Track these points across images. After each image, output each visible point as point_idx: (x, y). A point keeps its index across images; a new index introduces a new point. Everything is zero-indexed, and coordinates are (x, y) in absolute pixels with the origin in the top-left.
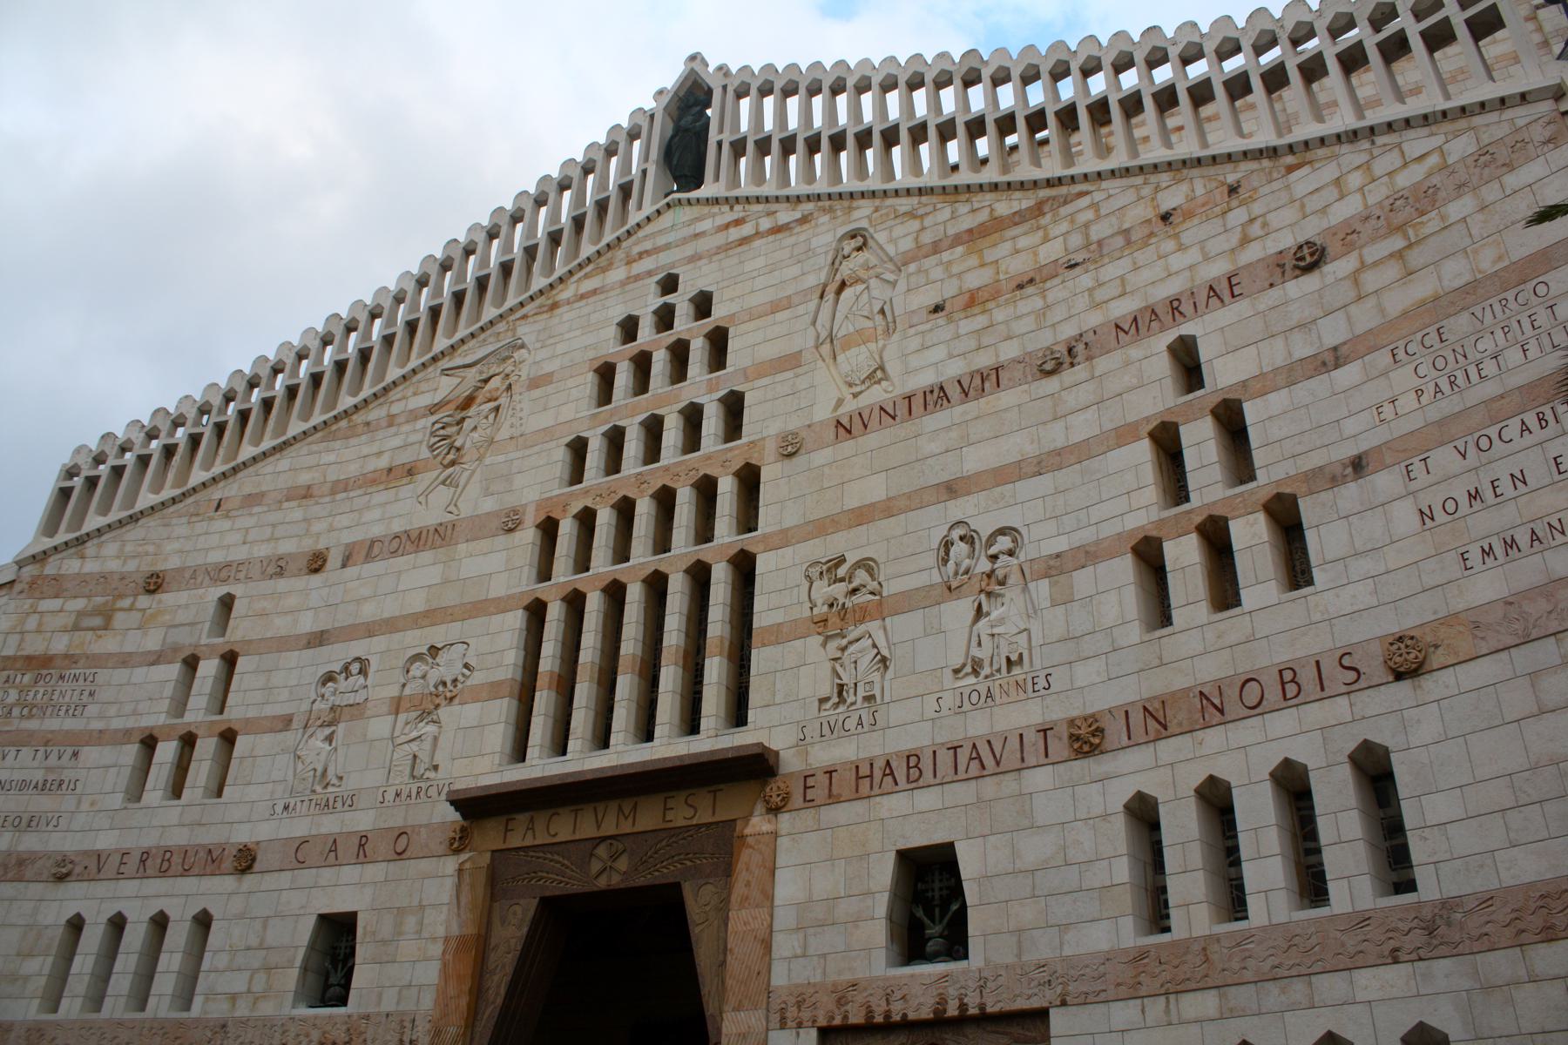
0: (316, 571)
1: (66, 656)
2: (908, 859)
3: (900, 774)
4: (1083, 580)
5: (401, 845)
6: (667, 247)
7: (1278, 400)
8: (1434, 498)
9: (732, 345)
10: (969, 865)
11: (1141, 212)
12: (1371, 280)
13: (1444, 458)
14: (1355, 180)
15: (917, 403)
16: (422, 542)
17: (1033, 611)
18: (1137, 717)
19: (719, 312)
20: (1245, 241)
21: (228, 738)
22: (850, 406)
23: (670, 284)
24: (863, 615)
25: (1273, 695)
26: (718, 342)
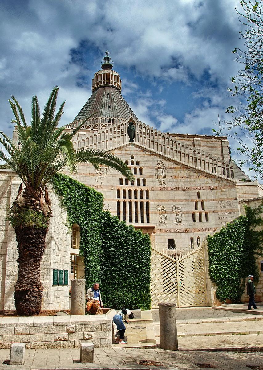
2: (169, 240)
3: (169, 231)
6: (132, 150)
8: (220, 217)
9: (144, 171)
10: (176, 241)
13: (221, 213)
14: (218, 182)
15: (169, 188)
16: (98, 187)
17: (182, 217)
18: (192, 230)
19: (141, 165)
20: (206, 183)
23: (132, 158)
26: (141, 170)
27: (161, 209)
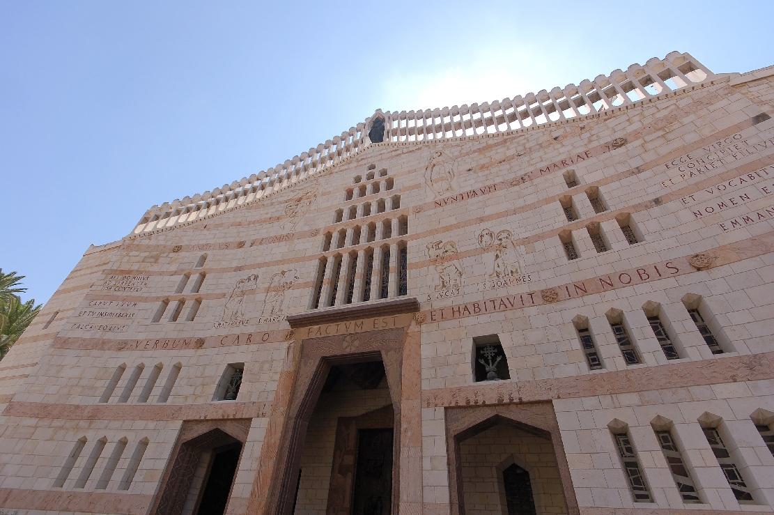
0: (240, 247)
1: (137, 271)
3: (471, 310)
4: (539, 245)
5: (265, 338)
7: (614, 185)
11: (546, 137)
12: (649, 146)
13: (700, 195)
15: (465, 196)
18: (572, 289)
19: (390, 174)
20: (590, 141)
21: (199, 301)
22: (439, 198)
24: (451, 259)
25: (636, 278)
26: (390, 184)
27: (443, 250)
